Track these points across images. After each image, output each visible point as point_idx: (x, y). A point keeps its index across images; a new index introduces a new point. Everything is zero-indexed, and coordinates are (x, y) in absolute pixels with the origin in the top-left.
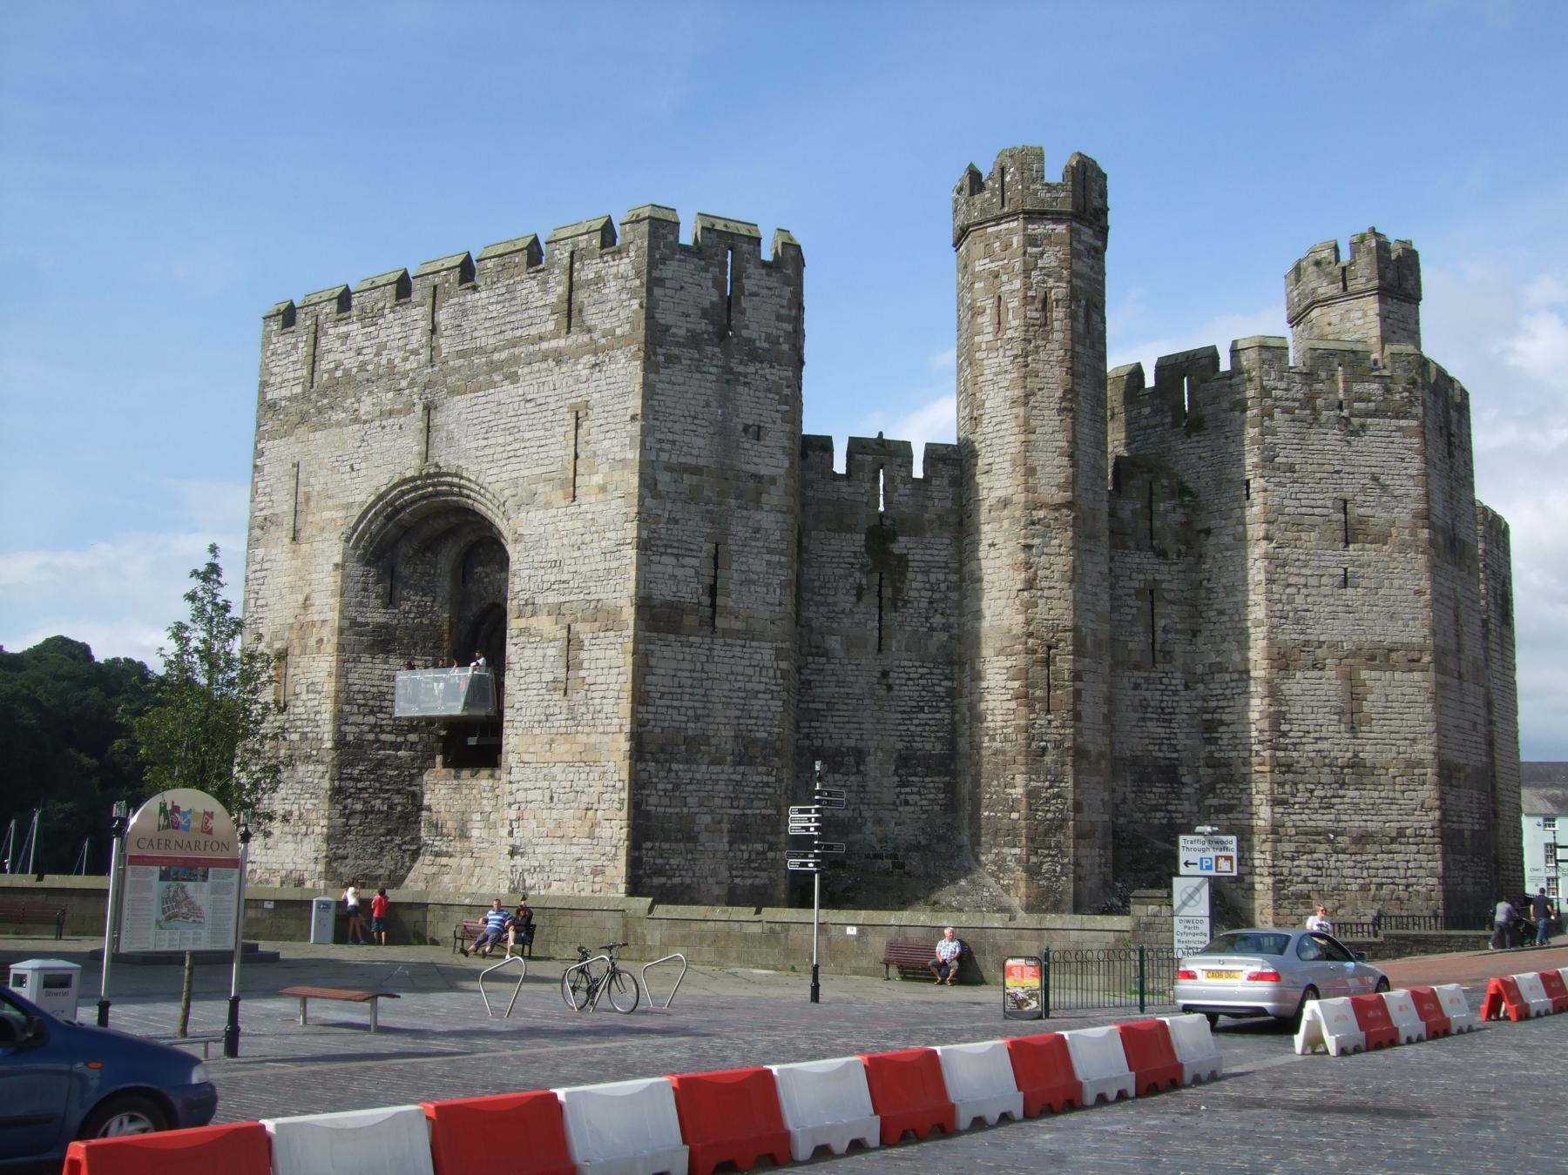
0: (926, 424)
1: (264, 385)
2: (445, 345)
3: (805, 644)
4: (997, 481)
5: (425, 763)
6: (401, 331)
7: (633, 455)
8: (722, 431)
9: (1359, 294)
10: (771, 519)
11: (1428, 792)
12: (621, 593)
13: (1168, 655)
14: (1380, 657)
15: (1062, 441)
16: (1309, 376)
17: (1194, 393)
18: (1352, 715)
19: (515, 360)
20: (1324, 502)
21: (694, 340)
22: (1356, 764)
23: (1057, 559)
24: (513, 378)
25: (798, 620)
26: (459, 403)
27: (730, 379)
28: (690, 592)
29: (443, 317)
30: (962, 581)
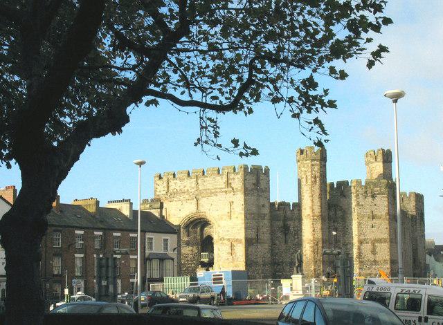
0: (292, 199)
1: (155, 191)
2: (201, 188)
3: (273, 243)
4: (306, 211)
5: (196, 267)
6: (189, 184)
7: (243, 212)
8: (258, 206)
9: (379, 162)
10: (266, 222)
11: (388, 266)
12: (242, 236)
13: (340, 241)
14: (380, 241)
15: (319, 204)
16: (366, 187)
17: (342, 189)
18: (374, 252)
19: (217, 192)
20: (369, 212)
21: (252, 190)
22: (375, 261)
23: (319, 226)
24: (217, 195)
25: (272, 239)
26: (204, 199)
27: (259, 196)
28: (254, 236)
29: (199, 181)
30: (299, 231)
